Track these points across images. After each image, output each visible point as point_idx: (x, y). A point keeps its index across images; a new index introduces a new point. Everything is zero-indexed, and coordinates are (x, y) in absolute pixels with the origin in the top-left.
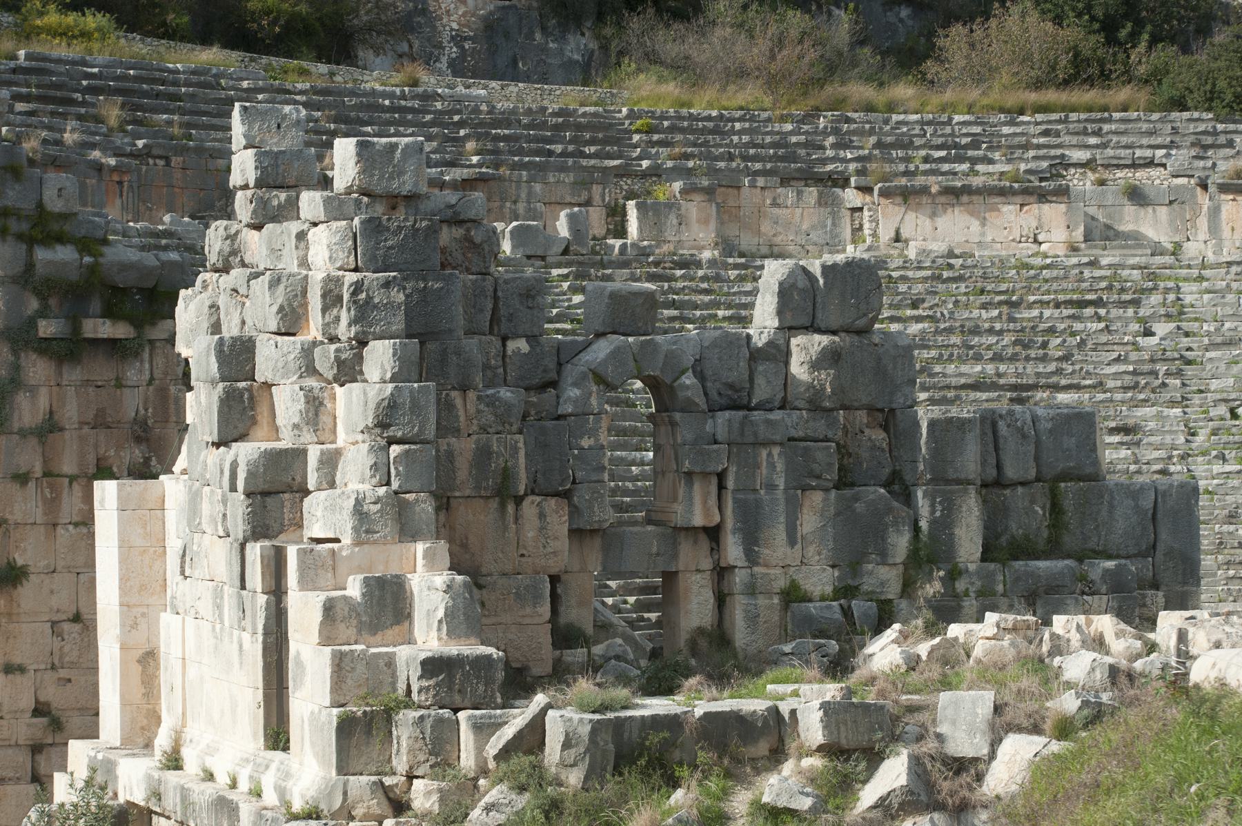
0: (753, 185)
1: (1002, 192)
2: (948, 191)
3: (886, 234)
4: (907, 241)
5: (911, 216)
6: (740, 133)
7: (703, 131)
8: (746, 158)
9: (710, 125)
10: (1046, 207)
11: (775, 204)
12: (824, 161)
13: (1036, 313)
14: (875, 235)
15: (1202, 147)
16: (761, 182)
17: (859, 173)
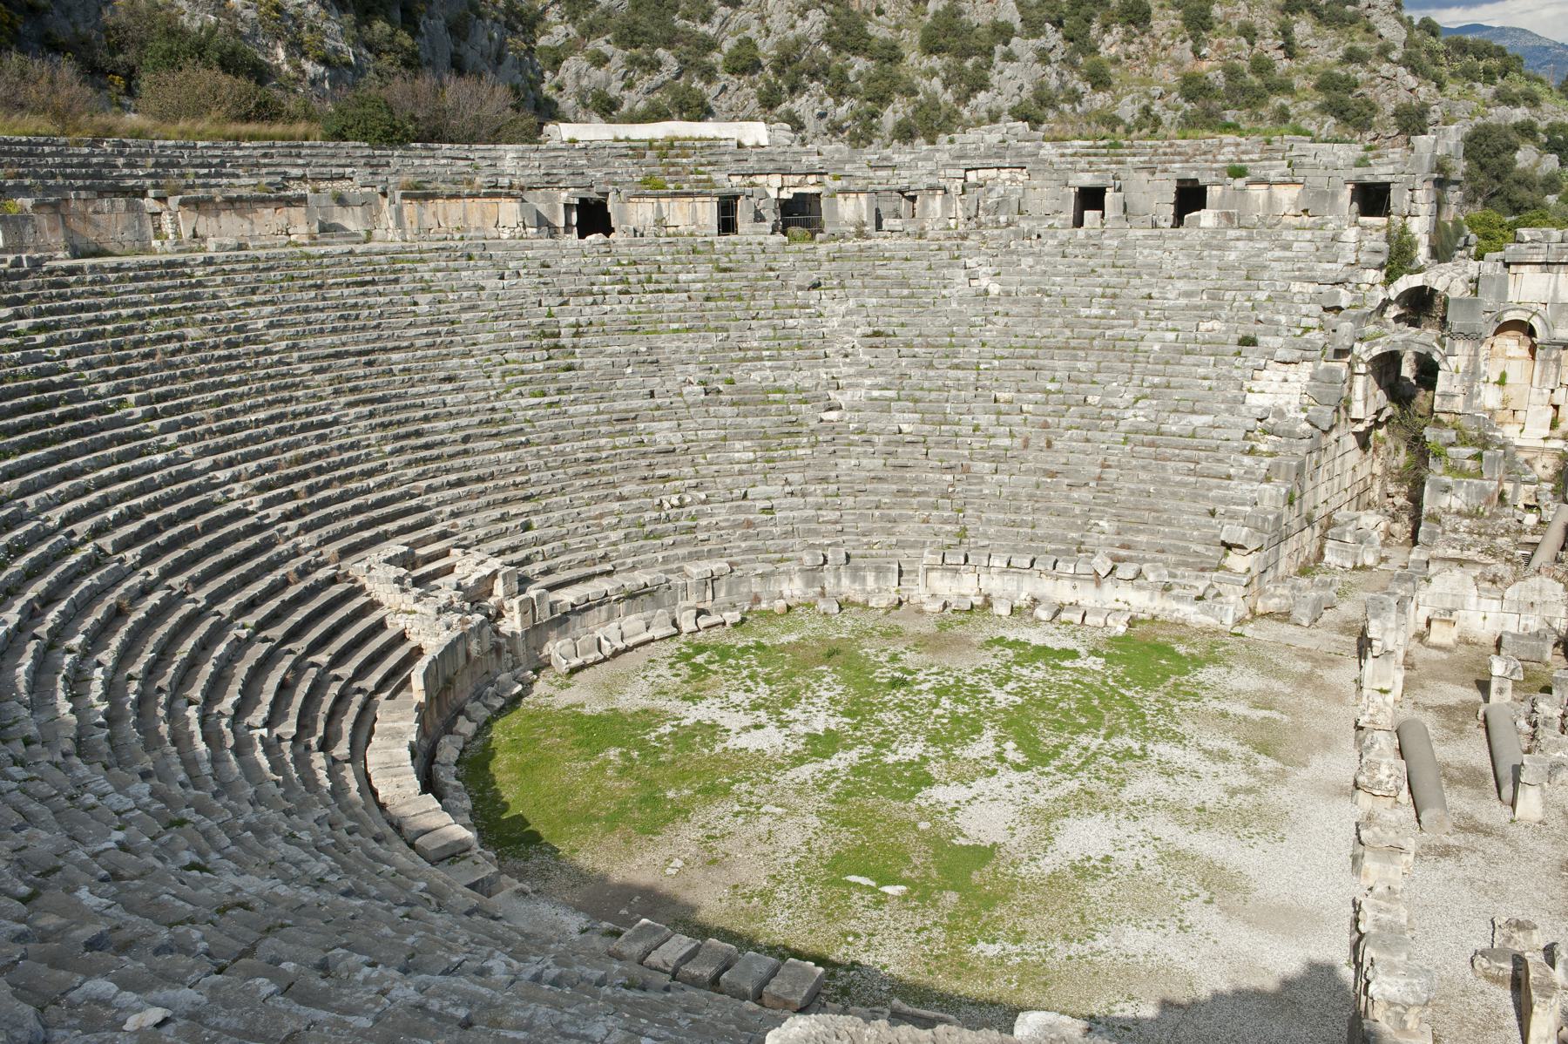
0: (78, 198)
1: (263, 201)
2: (230, 201)
3: (186, 234)
4: (204, 239)
5: (202, 219)
6: (51, 154)
7: (21, 154)
8: (66, 176)
9: (26, 148)
10: (292, 210)
11: (96, 212)
12: (123, 177)
13: (338, 292)
14: (177, 233)
15: (374, 166)
16: (83, 194)
17: (156, 186)
